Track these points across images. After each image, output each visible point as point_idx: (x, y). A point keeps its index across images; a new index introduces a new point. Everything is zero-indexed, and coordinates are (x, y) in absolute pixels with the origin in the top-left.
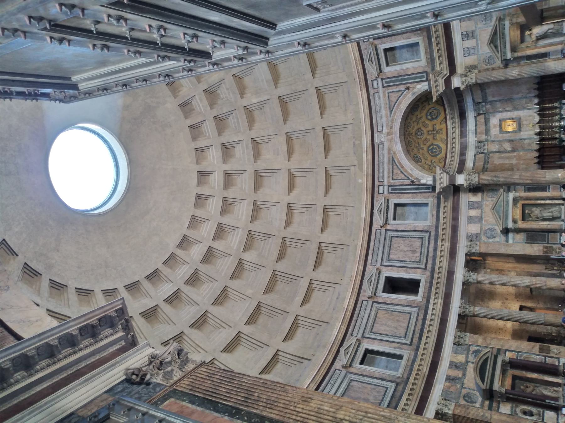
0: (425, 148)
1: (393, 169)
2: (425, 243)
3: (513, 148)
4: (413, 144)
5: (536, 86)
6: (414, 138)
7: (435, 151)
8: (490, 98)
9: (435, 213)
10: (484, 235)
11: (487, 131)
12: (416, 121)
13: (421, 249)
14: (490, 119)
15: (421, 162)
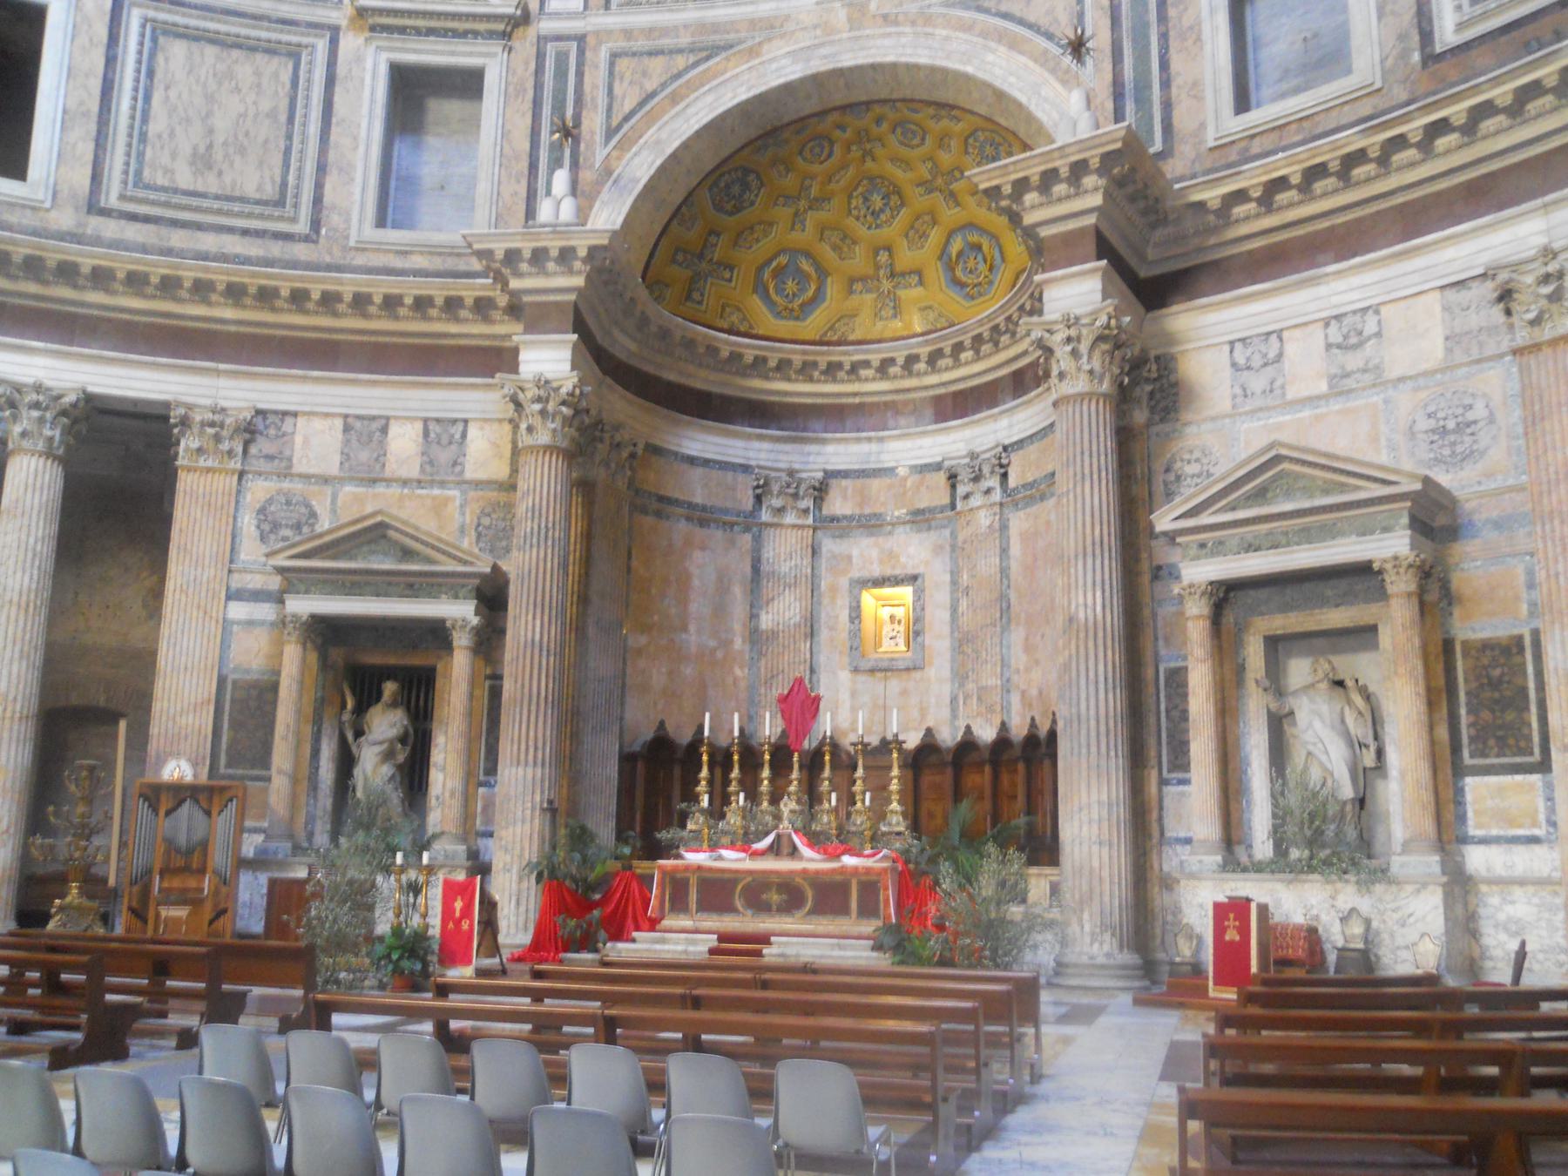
0: (804, 236)
1: (671, 52)
2: (250, 215)
3: (773, 634)
4: (817, 168)
5: (1043, 730)
6: (851, 172)
7: (791, 285)
8: (1019, 522)
9: (419, 262)
10: (279, 492)
11: (871, 524)
12: (936, 170)
13: (217, 197)
14: (925, 535)
15: (719, 208)
